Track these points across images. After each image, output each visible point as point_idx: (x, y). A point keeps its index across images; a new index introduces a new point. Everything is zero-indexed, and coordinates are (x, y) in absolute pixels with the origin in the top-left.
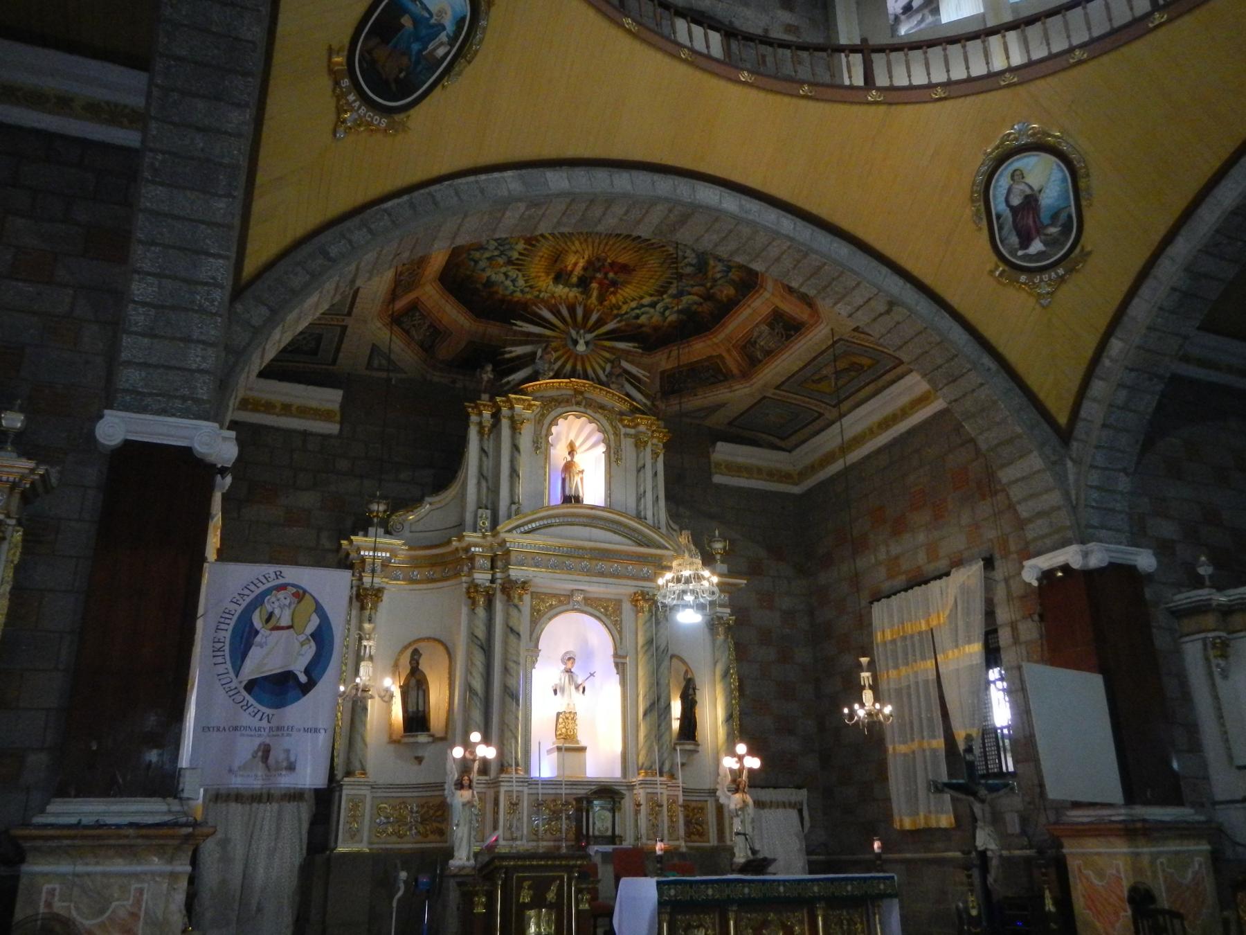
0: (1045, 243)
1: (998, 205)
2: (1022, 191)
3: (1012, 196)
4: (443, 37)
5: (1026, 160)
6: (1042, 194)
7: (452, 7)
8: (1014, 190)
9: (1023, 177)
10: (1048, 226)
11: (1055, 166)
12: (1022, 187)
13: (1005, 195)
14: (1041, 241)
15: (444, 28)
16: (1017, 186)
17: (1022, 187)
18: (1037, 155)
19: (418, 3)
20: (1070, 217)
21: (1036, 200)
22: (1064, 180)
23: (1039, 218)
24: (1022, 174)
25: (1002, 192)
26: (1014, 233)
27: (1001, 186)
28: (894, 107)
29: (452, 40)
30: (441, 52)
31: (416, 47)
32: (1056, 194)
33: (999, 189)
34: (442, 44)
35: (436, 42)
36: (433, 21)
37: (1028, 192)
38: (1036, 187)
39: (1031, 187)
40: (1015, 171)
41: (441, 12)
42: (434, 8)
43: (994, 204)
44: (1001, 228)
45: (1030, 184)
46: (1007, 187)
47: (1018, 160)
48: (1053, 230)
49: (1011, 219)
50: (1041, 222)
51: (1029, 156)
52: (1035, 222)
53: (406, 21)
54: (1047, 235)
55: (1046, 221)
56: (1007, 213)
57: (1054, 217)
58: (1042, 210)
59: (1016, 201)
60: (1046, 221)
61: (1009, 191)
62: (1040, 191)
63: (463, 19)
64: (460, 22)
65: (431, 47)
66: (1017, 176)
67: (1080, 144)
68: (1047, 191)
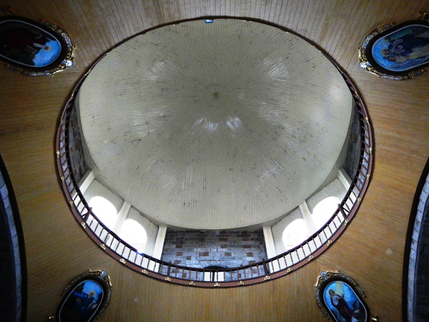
0: (356, 318)
1: (331, 307)
2: (336, 298)
3: (334, 302)
4: (94, 301)
5: (331, 286)
6: (344, 297)
7: (96, 291)
8: (333, 299)
9: (334, 293)
10: (354, 310)
11: (344, 285)
12: (335, 297)
13: (331, 302)
14: (355, 318)
15: (94, 299)
16: (333, 297)
17: (335, 297)
18: (335, 282)
19: (82, 293)
20: (360, 303)
21: (344, 300)
22: (349, 289)
23: (348, 307)
24: (333, 291)
25: (329, 301)
26: (342, 317)
27: (328, 299)
28: (275, 280)
29: (98, 302)
30: (94, 306)
31: (83, 308)
32: (349, 296)
33: (328, 300)
34: (94, 304)
35: (91, 304)
36: (89, 297)
37: (339, 298)
38: (341, 295)
39: (339, 296)
40: (330, 291)
41: (92, 294)
42: (89, 294)
43: (329, 307)
44: (336, 316)
45: (338, 294)
46: (330, 298)
47: (329, 286)
48: (357, 311)
49: (338, 311)
50: (351, 310)
51: (332, 284)
52: (348, 310)
53: (78, 300)
54: (355, 314)
55: (352, 308)
56: (335, 309)
57: (354, 305)
58: (348, 304)
59: (336, 303)
60: (352, 308)
61: (332, 299)
62: (343, 296)
63: (101, 294)
64: (100, 295)
65: (89, 306)
66: (332, 293)
67: (348, 274)
68: (346, 295)
